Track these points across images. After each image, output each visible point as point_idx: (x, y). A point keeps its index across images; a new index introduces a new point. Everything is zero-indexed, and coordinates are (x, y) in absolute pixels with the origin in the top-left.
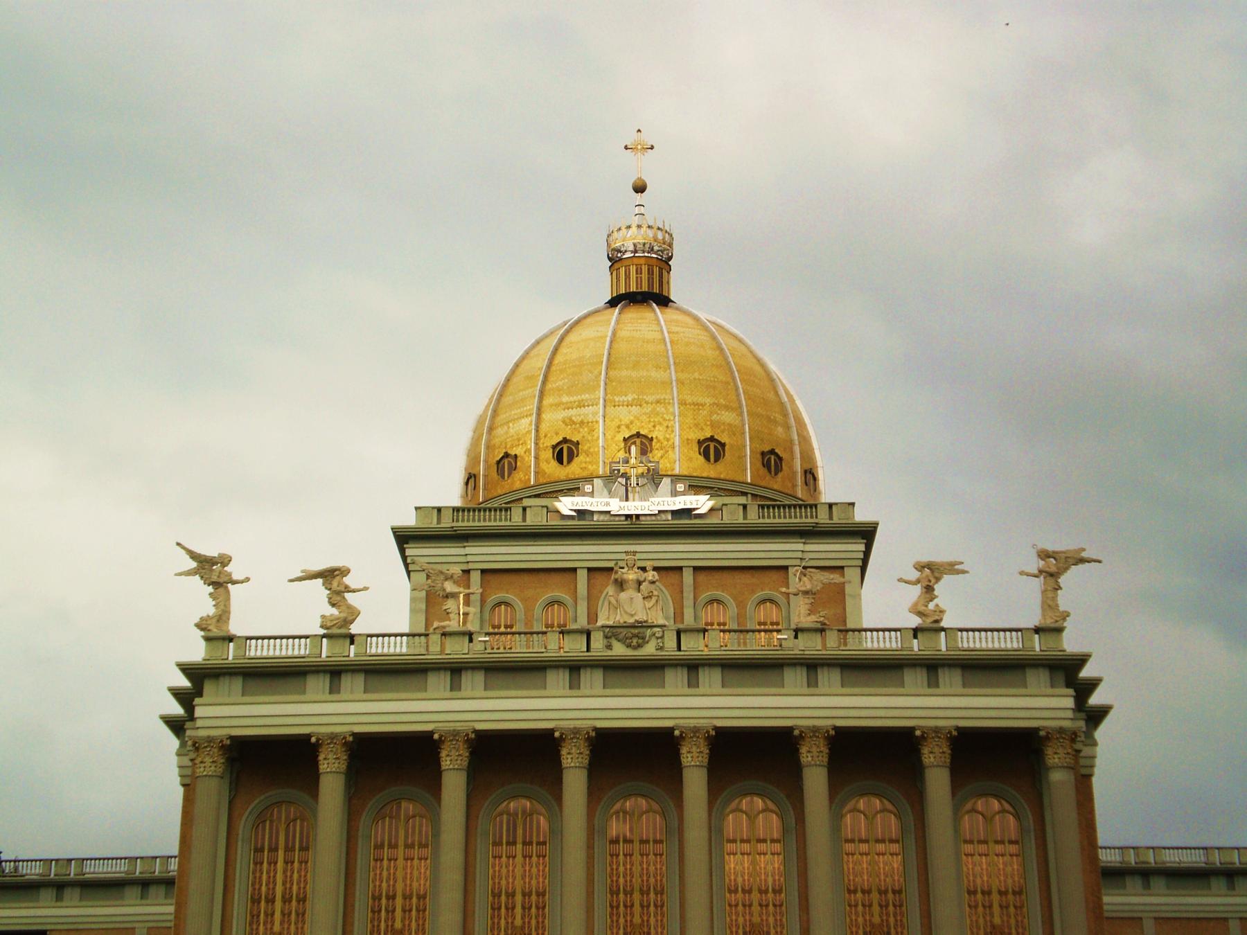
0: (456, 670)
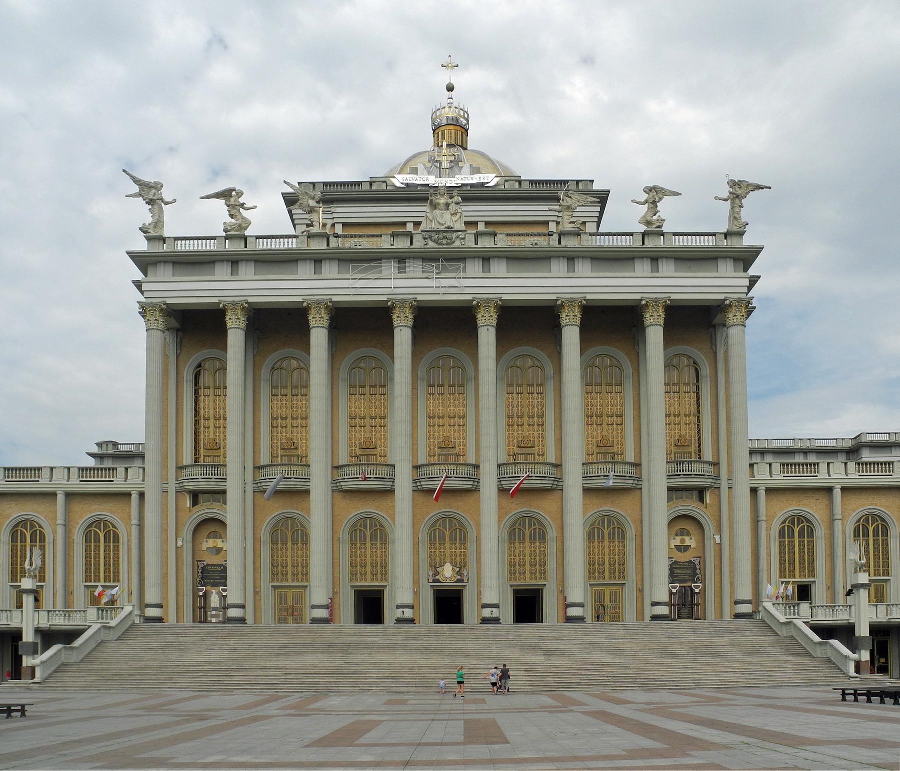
0: (318, 260)
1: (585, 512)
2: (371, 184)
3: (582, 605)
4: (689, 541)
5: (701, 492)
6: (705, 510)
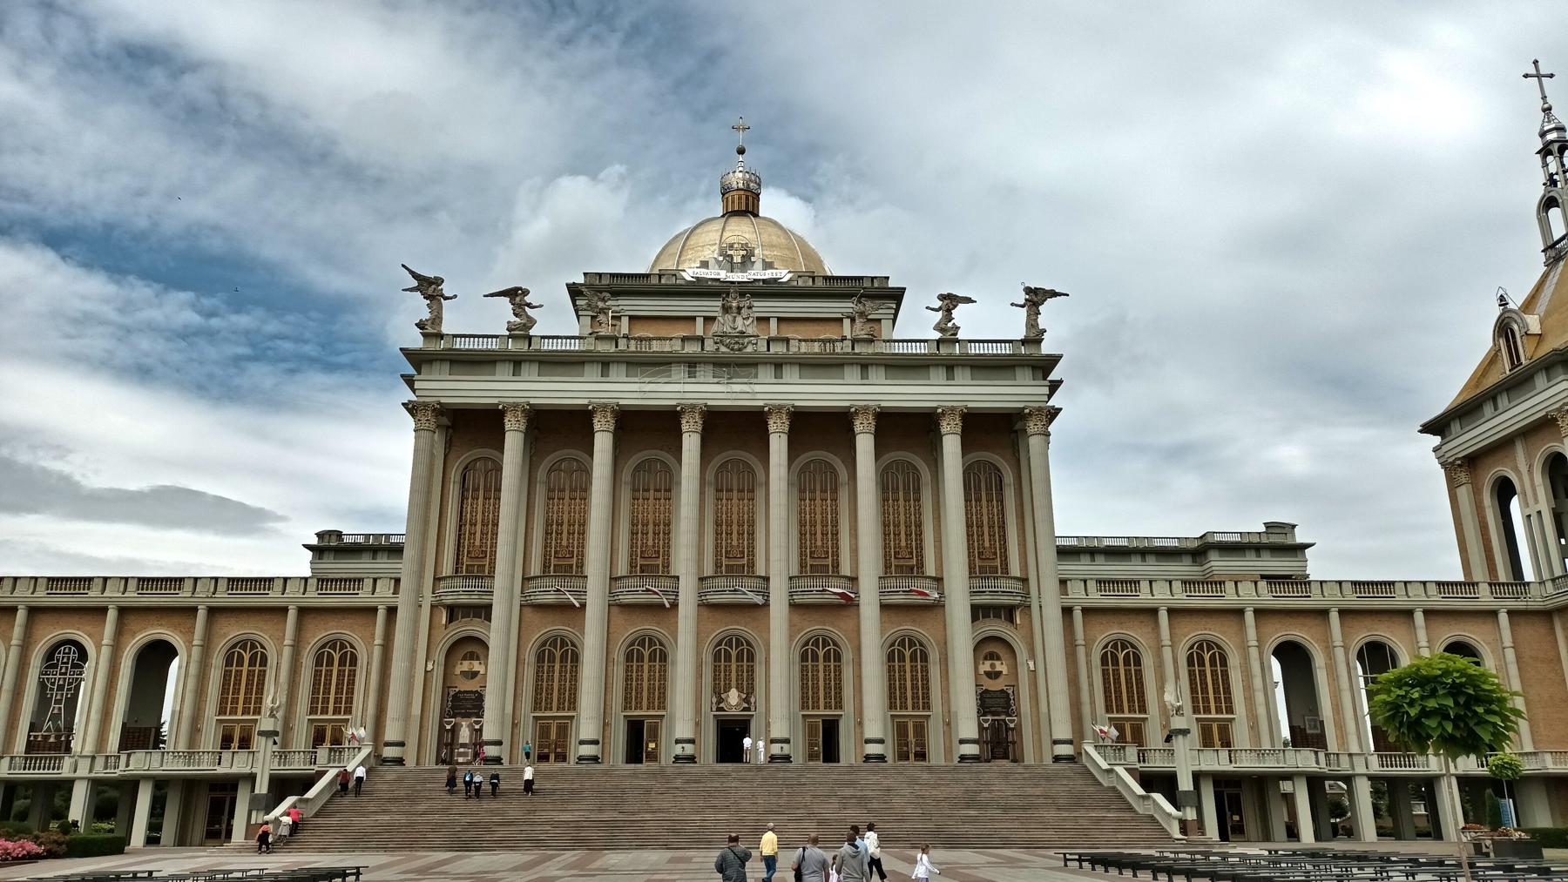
1: (882, 632)
2: (660, 276)
4: (1001, 667)
5: (1008, 613)
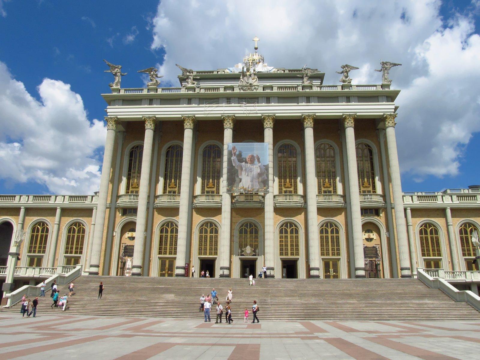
3: (318, 269)
5: (376, 211)
6: (378, 218)
